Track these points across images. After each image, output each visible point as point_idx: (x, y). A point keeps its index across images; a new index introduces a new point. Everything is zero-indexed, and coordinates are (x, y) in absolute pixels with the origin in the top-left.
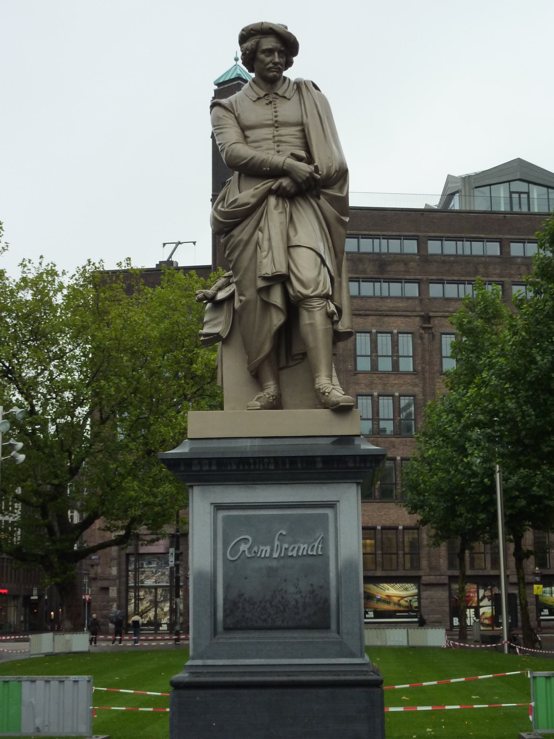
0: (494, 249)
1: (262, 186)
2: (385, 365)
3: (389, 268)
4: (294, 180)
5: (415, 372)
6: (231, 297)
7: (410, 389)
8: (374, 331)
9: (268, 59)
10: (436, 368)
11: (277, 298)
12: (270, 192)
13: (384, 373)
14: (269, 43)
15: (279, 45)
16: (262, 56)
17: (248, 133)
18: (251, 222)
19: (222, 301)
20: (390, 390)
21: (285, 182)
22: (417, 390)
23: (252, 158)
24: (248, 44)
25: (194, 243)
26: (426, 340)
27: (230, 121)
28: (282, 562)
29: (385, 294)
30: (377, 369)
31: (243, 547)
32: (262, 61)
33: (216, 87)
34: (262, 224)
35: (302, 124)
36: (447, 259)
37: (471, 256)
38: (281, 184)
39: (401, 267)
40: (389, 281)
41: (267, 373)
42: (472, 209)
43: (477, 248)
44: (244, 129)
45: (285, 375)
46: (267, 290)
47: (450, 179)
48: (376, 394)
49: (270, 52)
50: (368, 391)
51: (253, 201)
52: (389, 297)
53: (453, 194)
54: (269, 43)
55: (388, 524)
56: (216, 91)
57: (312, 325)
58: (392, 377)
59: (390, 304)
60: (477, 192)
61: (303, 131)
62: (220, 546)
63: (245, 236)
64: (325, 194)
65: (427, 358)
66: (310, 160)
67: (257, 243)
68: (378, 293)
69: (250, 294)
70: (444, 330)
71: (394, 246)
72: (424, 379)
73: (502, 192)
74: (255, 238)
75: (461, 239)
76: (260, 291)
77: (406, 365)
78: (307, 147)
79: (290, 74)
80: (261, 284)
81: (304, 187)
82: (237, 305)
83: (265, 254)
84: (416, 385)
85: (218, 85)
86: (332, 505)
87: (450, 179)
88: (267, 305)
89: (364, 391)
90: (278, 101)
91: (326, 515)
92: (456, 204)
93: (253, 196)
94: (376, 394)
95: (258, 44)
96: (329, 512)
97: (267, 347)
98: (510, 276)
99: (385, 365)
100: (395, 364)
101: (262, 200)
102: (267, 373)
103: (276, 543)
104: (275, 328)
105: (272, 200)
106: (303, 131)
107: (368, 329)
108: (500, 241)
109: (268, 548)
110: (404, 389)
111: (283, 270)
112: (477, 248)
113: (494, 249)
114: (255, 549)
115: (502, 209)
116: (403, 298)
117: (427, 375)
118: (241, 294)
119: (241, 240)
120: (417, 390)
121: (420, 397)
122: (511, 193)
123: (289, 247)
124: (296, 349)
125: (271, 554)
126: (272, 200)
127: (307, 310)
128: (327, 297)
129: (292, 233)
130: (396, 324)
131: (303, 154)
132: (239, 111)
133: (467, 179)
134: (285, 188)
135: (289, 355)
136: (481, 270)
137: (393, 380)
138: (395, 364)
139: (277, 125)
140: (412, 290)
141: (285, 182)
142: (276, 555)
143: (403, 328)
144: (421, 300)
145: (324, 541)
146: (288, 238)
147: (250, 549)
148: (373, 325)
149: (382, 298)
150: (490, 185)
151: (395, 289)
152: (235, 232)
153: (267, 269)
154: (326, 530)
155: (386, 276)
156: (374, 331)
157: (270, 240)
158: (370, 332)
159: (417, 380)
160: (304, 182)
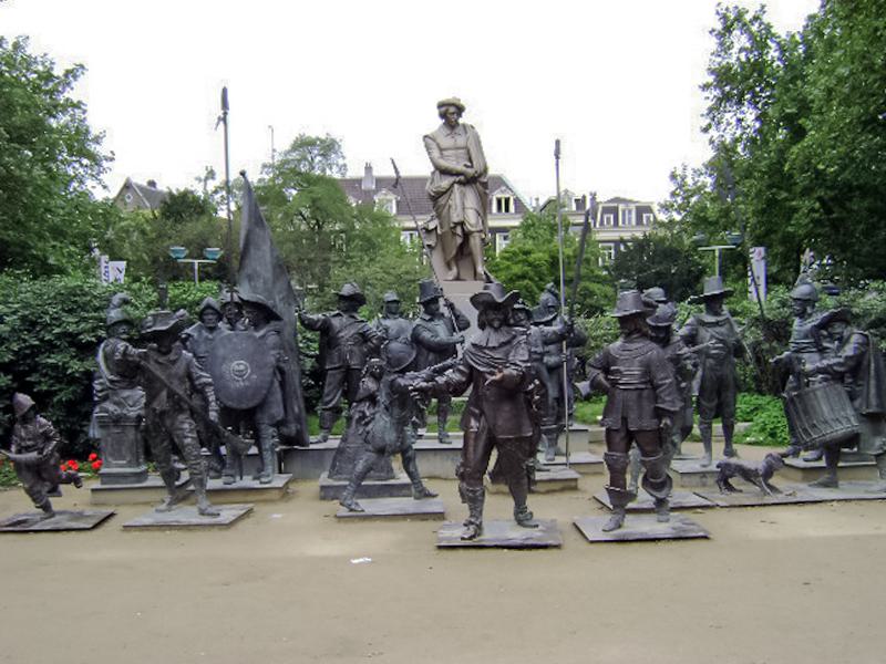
1: (452, 179)
6: (436, 228)
11: (459, 230)
12: (455, 182)
14: (452, 109)
18: (447, 196)
21: (462, 178)
24: (443, 109)
27: (434, 146)
41: (453, 264)
44: (441, 150)
45: (460, 263)
46: (455, 227)
54: (452, 109)
57: (475, 244)
66: (472, 167)
69: (446, 229)
78: (470, 160)
79: (461, 121)
80: (452, 225)
82: (439, 232)
88: (455, 234)
97: (454, 252)
101: (452, 185)
102: (453, 264)
105: (456, 186)
118: (442, 228)
124: (465, 252)
126: (456, 186)
128: (481, 231)
131: (469, 164)
132: (439, 141)
135: (462, 254)
141: (462, 178)
153: (456, 220)
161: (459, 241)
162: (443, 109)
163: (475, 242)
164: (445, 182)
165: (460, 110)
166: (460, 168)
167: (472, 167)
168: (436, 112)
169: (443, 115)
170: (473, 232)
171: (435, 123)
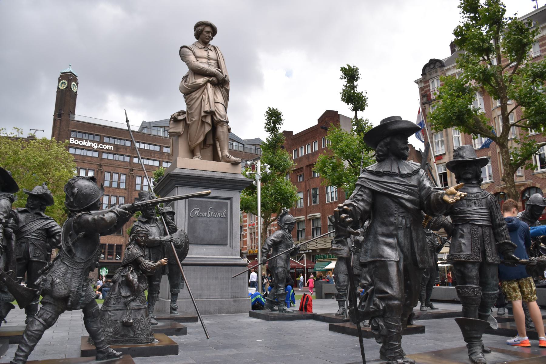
0: (157, 149)
2: (115, 185)
3: (120, 150)
4: (218, 79)
5: (126, 189)
6: (185, 120)
7: (123, 195)
8: (112, 172)
9: (207, 35)
10: (133, 188)
11: (209, 120)
12: (208, 81)
13: (114, 188)
15: (212, 31)
16: (205, 33)
17: (198, 59)
19: (181, 120)
20: (116, 194)
21: (214, 79)
22: (126, 195)
23: (203, 68)
24: (200, 28)
25: (43, 131)
26: (130, 178)
28: (210, 219)
29: (117, 159)
30: (112, 186)
31: (196, 212)
32: (205, 35)
33: (61, 74)
34: (205, 92)
35: (217, 61)
36: (141, 150)
37: (149, 150)
38: (213, 79)
39: (125, 150)
40: (119, 155)
41: (198, 149)
42: (151, 133)
43: (152, 148)
46: (205, 117)
47: (144, 122)
48: (110, 195)
49: (208, 32)
50: (107, 194)
51: (202, 83)
52: (119, 161)
53: (146, 127)
54: (208, 29)
55: (111, 243)
56: (60, 75)
58: (117, 190)
59: (119, 163)
60: (153, 128)
61: (218, 63)
62: (187, 211)
63: (197, 95)
64: (224, 88)
65: (130, 184)
66: (222, 73)
67: (202, 99)
68: (115, 159)
69: (196, 118)
70: (137, 175)
71: (123, 143)
72: (129, 191)
73: (162, 129)
74: (201, 97)
75: (147, 144)
76: (203, 116)
77: (123, 186)
79: (211, 43)
80: (203, 114)
81: (220, 82)
83: (206, 103)
84: (125, 193)
85: (62, 73)
86: (229, 199)
87: (144, 122)
89: (106, 194)
90: (209, 51)
91: (227, 204)
92: (145, 131)
93: (203, 81)
94: (110, 195)
95: (204, 28)
96: (228, 201)
97: (202, 139)
98: (162, 159)
99: (115, 185)
100: (119, 185)
101: (206, 84)
102: (198, 149)
103: (209, 211)
104: (206, 132)
105: (209, 85)
106: (218, 63)
107: (110, 171)
108: (160, 146)
109: (206, 213)
110: (121, 194)
111: (214, 110)
112: (152, 148)
113: (157, 149)
114: (201, 213)
115: (161, 135)
116: (123, 162)
117: (130, 190)
119: (196, 97)
120: (126, 195)
121: (127, 198)
122: (165, 130)
123: (215, 103)
125: (207, 215)
127: (221, 126)
129: (216, 98)
130: (120, 171)
133: (150, 123)
134: (214, 81)
136: (152, 155)
137: (117, 191)
138: (119, 185)
139: (209, 58)
140: (127, 159)
142: (209, 216)
143: (123, 172)
144: (130, 163)
145: (227, 212)
146: (215, 100)
147: (199, 213)
148: (112, 170)
149: (116, 160)
150: (158, 127)
151: (121, 158)
152: (193, 94)
154: (227, 209)
155: (118, 153)
156: (112, 172)
157: (208, 98)
158: (110, 172)
159: (126, 192)
160: (221, 80)
161: (208, 129)
162: (200, 28)
163: (221, 130)
164: (201, 81)
165: (214, 31)
166: (214, 69)
167: (222, 73)
168: (193, 32)
169: (198, 35)
170: (223, 121)
171: (190, 39)
